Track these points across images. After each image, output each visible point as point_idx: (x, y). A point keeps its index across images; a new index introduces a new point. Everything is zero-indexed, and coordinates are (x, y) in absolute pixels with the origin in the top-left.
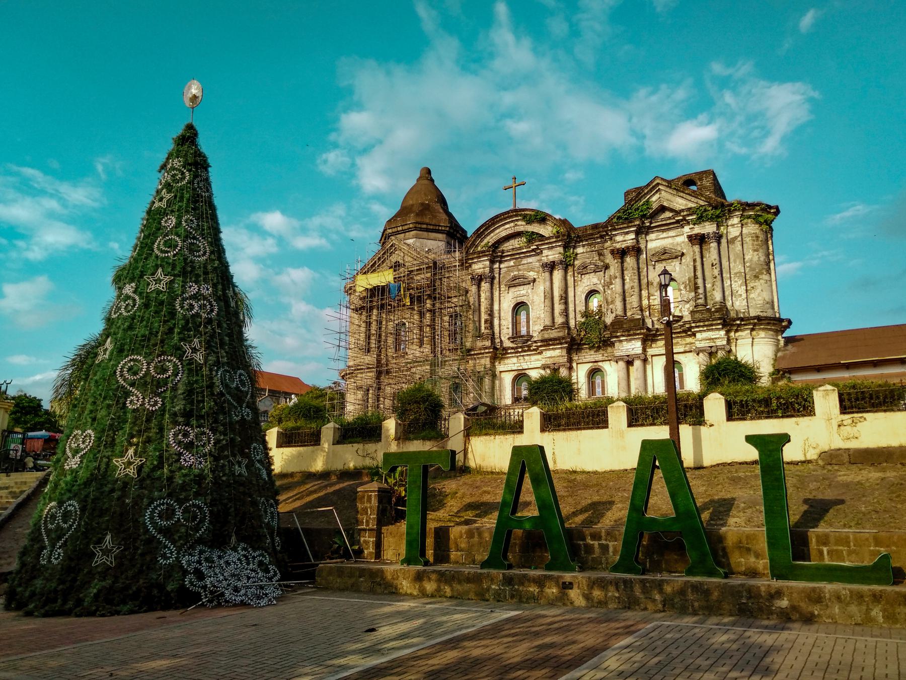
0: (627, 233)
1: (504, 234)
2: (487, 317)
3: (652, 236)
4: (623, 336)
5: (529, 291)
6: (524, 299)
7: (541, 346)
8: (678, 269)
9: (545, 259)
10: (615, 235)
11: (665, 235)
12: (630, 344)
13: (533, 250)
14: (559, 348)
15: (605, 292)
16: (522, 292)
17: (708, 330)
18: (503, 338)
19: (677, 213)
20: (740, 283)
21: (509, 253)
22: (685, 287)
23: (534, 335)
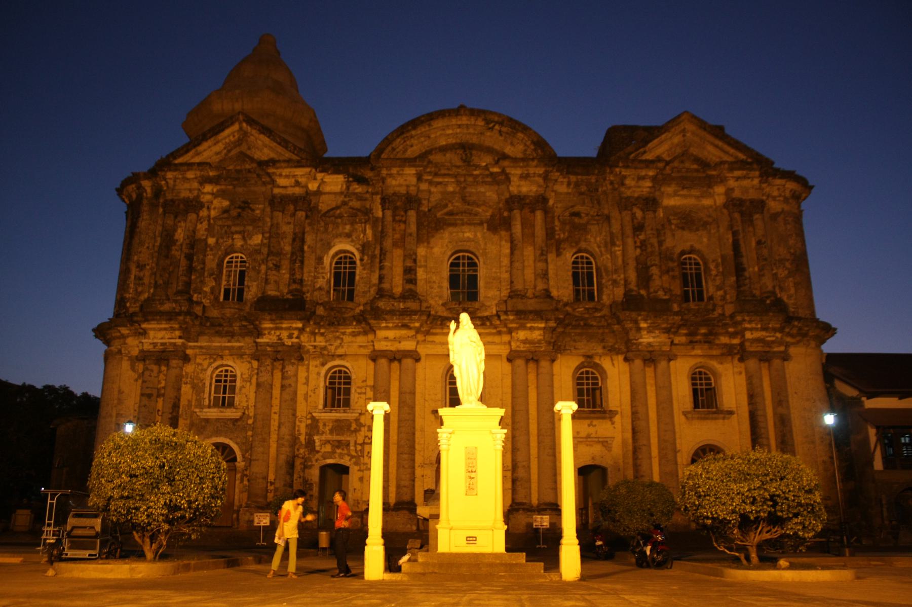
0: (641, 178)
1: (443, 142)
2: (409, 264)
3: (670, 190)
4: (645, 320)
5: (479, 235)
6: (471, 246)
7: (512, 321)
8: (705, 240)
9: (514, 189)
10: (625, 177)
11: (685, 192)
12: (653, 335)
13: (492, 174)
14: (539, 329)
15: (602, 255)
16: (467, 235)
17: (764, 329)
18: (432, 302)
19: (704, 164)
20: (786, 272)
21: (451, 172)
22: (717, 266)
23: (488, 304)
